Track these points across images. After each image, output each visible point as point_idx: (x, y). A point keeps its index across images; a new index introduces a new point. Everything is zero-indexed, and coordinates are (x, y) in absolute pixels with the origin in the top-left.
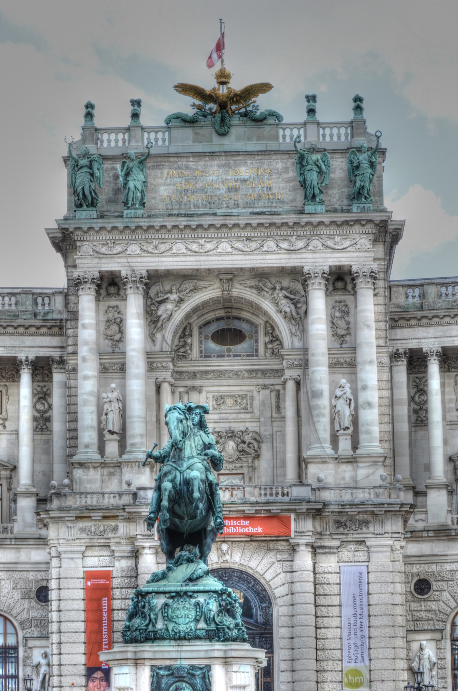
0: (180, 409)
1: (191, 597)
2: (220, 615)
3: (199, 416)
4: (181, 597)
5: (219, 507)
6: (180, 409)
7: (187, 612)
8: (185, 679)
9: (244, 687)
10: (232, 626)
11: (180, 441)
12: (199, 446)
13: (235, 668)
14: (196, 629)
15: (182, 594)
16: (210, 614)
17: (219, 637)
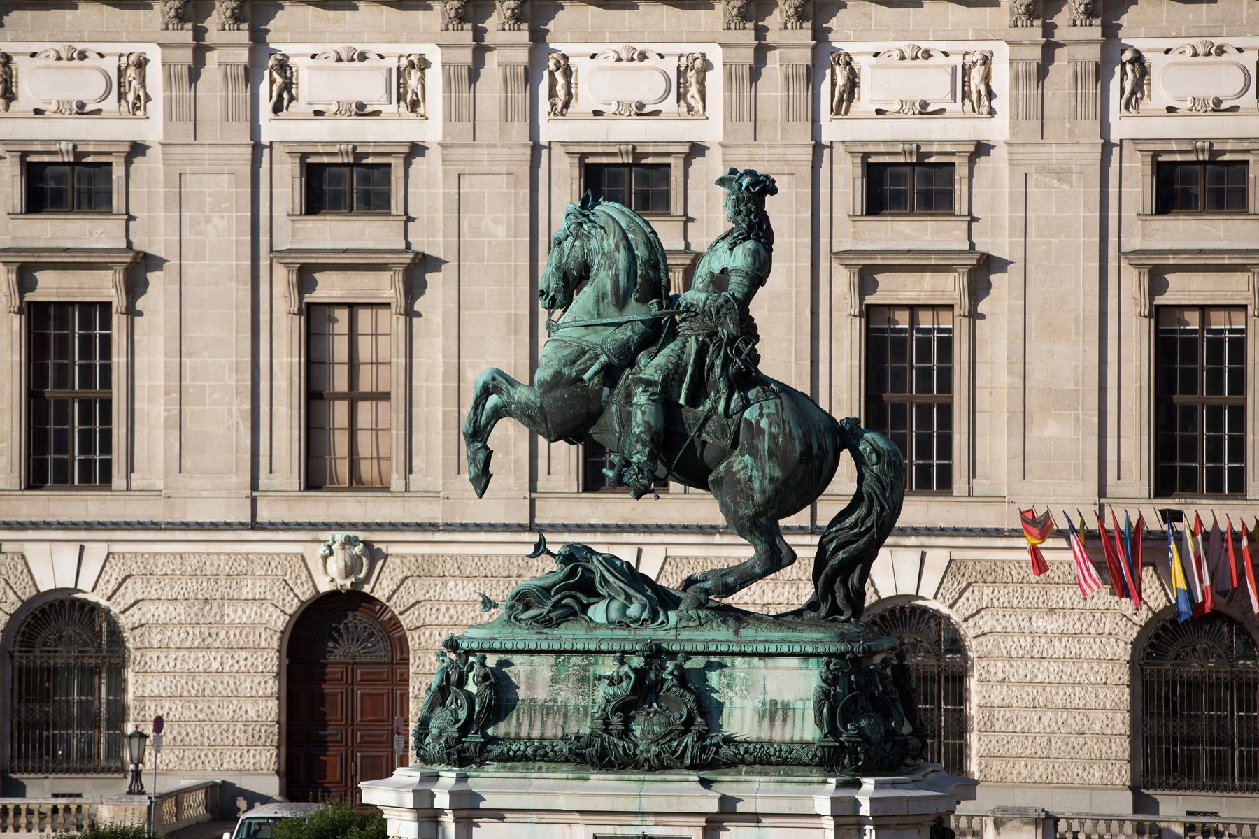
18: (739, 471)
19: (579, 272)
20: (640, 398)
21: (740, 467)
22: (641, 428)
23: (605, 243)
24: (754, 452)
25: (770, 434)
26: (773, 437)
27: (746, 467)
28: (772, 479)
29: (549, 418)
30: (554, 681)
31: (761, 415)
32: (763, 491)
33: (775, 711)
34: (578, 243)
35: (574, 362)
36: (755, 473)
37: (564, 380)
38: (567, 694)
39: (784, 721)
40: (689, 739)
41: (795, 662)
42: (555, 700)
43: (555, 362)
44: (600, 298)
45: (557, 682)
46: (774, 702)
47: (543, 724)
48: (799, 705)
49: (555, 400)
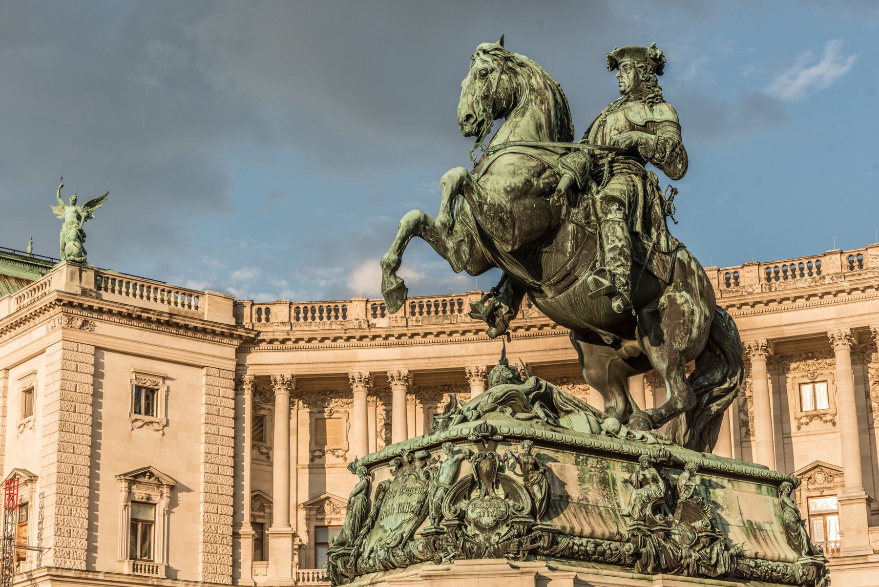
0: (485, 52)
2: (475, 494)
3: (631, 75)
6: (485, 52)
7: (404, 498)
19: (508, 104)
21: (683, 300)
22: (623, 243)
23: (533, 81)
25: (698, 276)
26: (701, 279)
27: (687, 301)
28: (705, 315)
29: (517, 224)
30: (581, 480)
31: (689, 257)
32: (699, 327)
33: (753, 530)
34: (504, 77)
35: (539, 175)
36: (696, 308)
37: (533, 190)
38: (594, 495)
40: (717, 548)
41: (751, 487)
43: (524, 171)
44: (539, 127)
45: (583, 482)
46: (750, 523)
48: (767, 527)
49: (525, 208)
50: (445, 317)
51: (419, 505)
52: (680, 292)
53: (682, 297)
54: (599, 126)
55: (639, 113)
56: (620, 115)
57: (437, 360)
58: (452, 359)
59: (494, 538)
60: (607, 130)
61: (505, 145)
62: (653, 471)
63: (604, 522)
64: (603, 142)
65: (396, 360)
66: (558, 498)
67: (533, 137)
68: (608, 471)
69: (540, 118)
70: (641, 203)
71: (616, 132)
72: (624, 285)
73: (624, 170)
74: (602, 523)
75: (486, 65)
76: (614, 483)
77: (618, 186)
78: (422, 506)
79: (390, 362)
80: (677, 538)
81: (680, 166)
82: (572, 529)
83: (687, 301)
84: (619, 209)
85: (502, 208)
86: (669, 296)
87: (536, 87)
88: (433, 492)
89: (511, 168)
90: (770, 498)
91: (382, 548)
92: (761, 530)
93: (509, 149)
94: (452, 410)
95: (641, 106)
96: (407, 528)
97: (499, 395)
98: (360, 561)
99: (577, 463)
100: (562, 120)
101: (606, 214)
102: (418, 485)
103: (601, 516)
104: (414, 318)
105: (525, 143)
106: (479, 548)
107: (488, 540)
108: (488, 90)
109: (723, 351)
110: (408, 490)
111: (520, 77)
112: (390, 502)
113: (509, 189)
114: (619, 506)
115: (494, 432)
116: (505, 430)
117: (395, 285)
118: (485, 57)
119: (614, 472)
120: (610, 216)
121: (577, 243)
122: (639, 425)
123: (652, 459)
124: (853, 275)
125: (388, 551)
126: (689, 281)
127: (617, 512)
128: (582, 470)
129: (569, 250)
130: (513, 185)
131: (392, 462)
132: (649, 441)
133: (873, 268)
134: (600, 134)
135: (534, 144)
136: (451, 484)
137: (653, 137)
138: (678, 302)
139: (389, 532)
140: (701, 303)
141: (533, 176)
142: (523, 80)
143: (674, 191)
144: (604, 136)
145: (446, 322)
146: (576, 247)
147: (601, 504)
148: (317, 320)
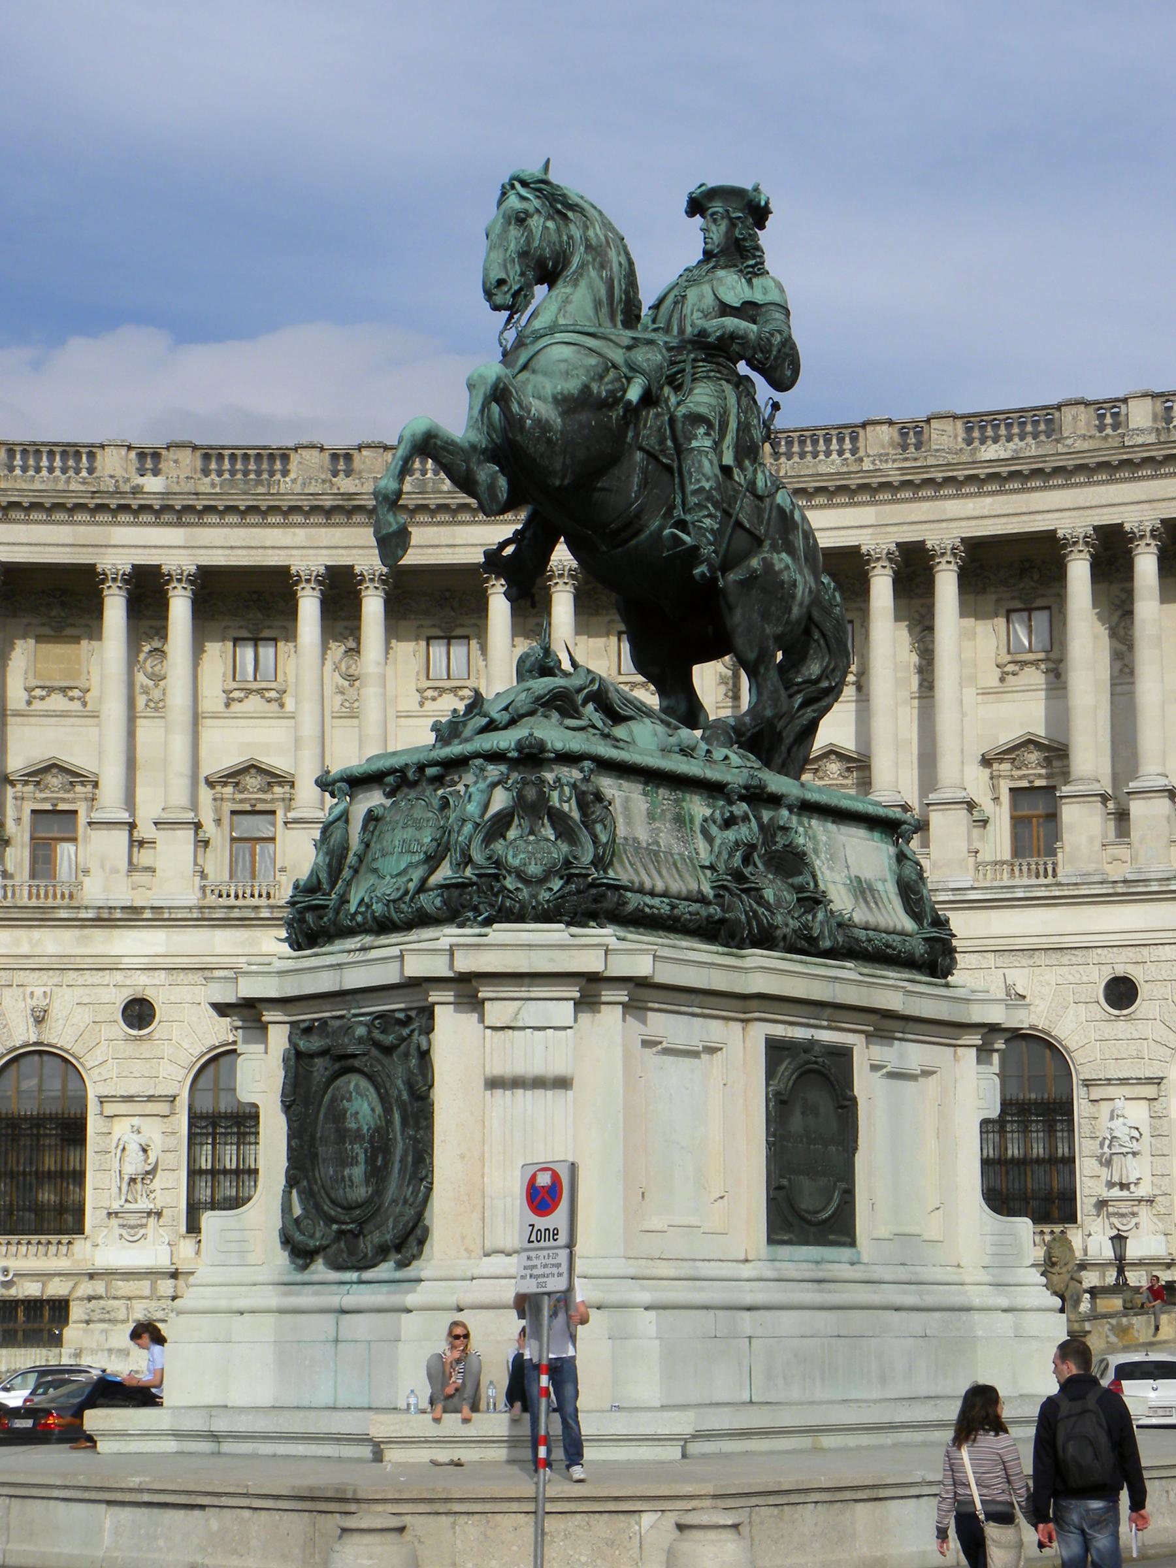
1: (438, 781)
2: (512, 834)
4: (414, 784)
5: (695, 492)
6: (524, 184)
7: (409, 833)
8: (357, 1063)
9: (562, 1083)
10: (534, 869)
11: (501, 282)
12: (697, 315)
13: (496, 1012)
14: (422, 888)
15: (410, 775)
16: (459, 832)
17: (475, 909)
18: (781, 571)
19: (555, 266)
20: (702, 441)
21: (782, 566)
23: (591, 233)
24: (791, 551)
27: (787, 567)
30: (651, 816)
32: (801, 605)
33: (862, 890)
34: (550, 224)
35: (601, 378)
36: (798, 577)
38: (667, 838)
39: (876, 904)
42: (657, 843)
43: (581, 371)
44: (597, 304)
47: (660, 873)
48: (879, 886)
50: (258, 482)
51: (434, 844)
52: (778, 553)
53: (781, 560)
54: (676, 303)
55: (734, 288)
56: (706, 289)
57: (244, 552)
58: (270, 552)
59: (544, 895)
60: (687, 310)
61: (553, 329)
62: (744, 806)
63: (680, 876)
64: (682, 331)
65: (177, 549)
66: (622, 841)
67: (590, 320)
68: (684, 804)
69: (599, 291)
70: (733, 425)
71: (701, 315)
72: (711, 544)
73: (712, 374)
74: (677, 876)
75: (525, 205)
76: (692, 821)
77: (705, 399)
78: (439, 845)
79: (166, 551)
80: (772, 901)
81: (788, 373)
82: (642, 884)
83: (787, 567)
84: (707, 434)
85: (550, 425)
86: (764, 559)
87: (594, 242)
88: (456, 829)
89: (563, 366)
90: (884, 846)
91: (379, 900)
92: (872, 890)
93: (559, 337)
94: (475, 711)
95: (736, 277)
96: (417, 875)
97: (541, 692)
98: (342, 916)
99: (645, 794)
100: (627, 293)
101: (690, 441)
102: (431, 814)
103: (677, 868)
104: (207, 480)
105: (581, 329)
106: (523, 907)
107: (534, 896)
108: (528, 242)
109: (824, 635)
110: (415, 821)
111: (572, 226)
112: (388, 836)
113: (559, 397)
114: (697, 854)
115: (541, 746)
116: (559, 746)
117: (394, 527)
118: (523, 192)
119: (691, 806)
120: (694, 444)
121: (646, 479)
122: (718, 740)
123: (743, 791)
124: (906, 459)
125: (387, 906)
126: (791, 537)
127: (695, 861)
128: (652, 803)
129: (636, 488)
130: (566, 392)
131: (390, 779)
132: (734, 765)
133: (937, 450)
134: (676, 316)
135: (592, 330)
136: (482, 816)
137: (754, 327)
138: (777, 568)
139: (388, 877)
140: (806, 571)
141: (593, 379)
142: (577, 233)
143: (776, 406)
144: (682, 319)
145: (261, 490)
146: (644, 484)
147: (676, 850)
148: (44, 473)
